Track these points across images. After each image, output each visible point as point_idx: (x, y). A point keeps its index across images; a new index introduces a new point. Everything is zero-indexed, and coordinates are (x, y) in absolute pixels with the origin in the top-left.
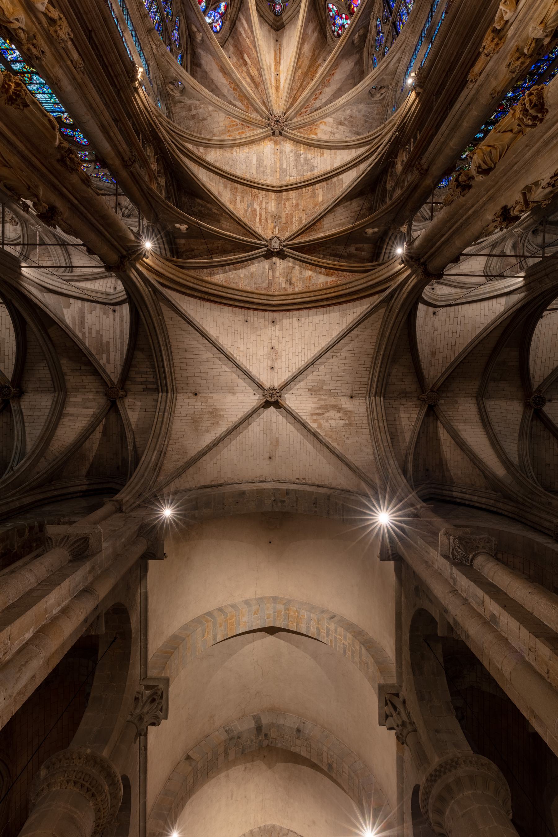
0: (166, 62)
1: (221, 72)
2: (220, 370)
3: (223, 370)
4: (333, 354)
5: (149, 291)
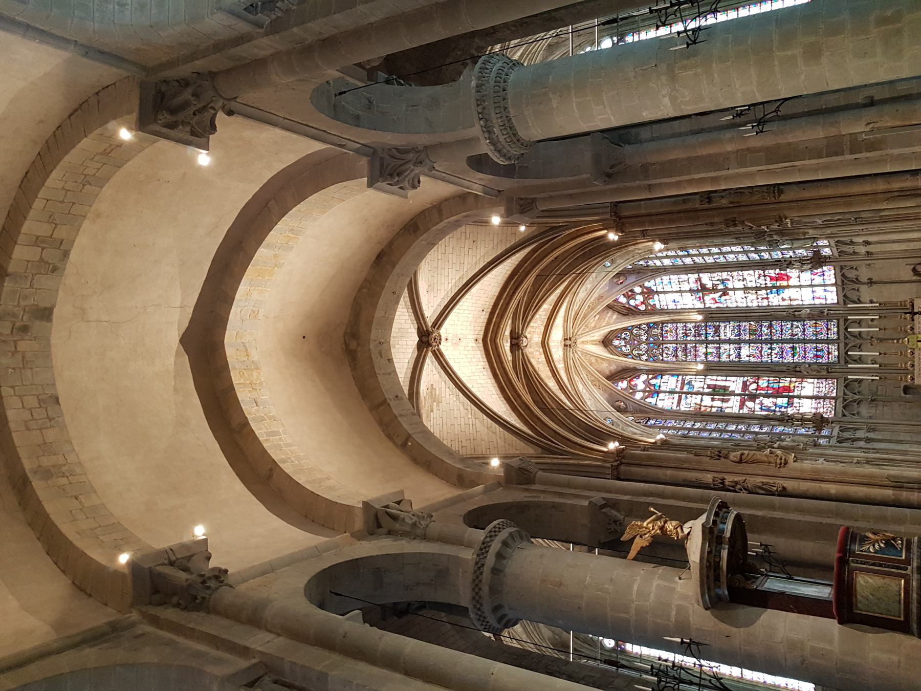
0: (627, 258)
1: (599, 296)
2: (450, 278)
3: (450, 281)
4: (469, 410)
5: (559, 223)
